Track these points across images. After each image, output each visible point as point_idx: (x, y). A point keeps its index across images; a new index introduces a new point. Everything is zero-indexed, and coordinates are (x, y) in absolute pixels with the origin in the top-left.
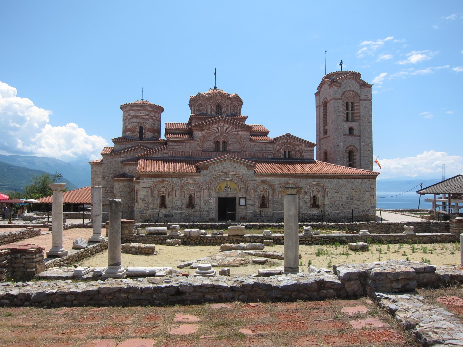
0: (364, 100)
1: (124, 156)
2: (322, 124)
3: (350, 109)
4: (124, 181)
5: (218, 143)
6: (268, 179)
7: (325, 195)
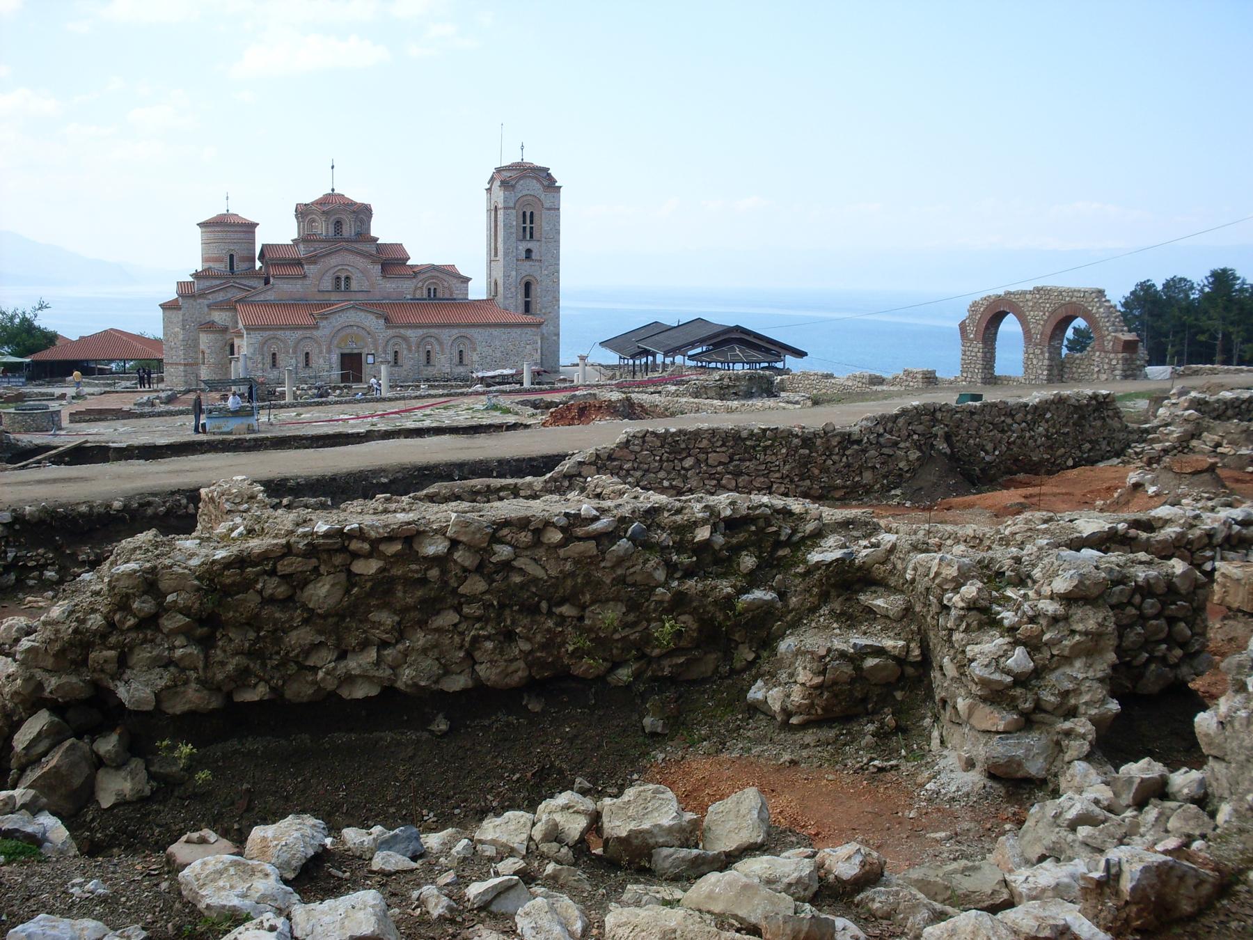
0: (549, 209)
1: (211, 299)
2: (493, 238)
3: (528, 221)
4: (212, 332)
5: (338, 278)
6: (402, 331)
7: (475, 350)
